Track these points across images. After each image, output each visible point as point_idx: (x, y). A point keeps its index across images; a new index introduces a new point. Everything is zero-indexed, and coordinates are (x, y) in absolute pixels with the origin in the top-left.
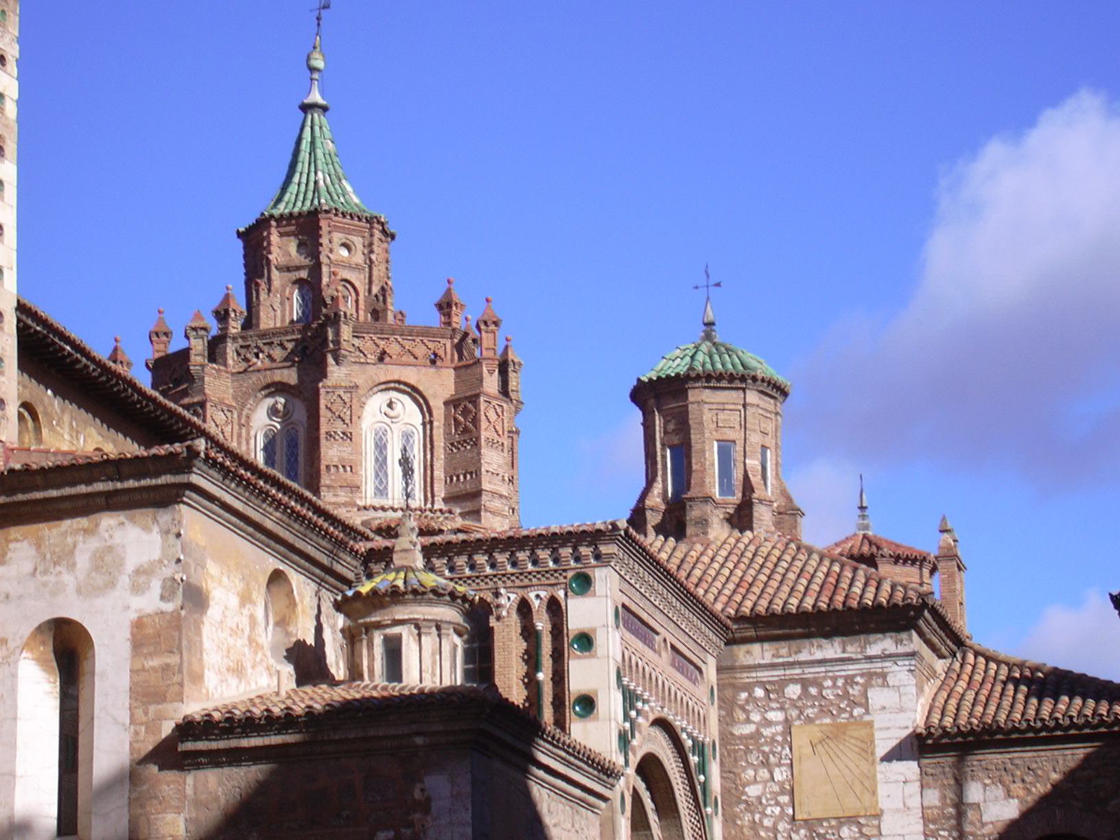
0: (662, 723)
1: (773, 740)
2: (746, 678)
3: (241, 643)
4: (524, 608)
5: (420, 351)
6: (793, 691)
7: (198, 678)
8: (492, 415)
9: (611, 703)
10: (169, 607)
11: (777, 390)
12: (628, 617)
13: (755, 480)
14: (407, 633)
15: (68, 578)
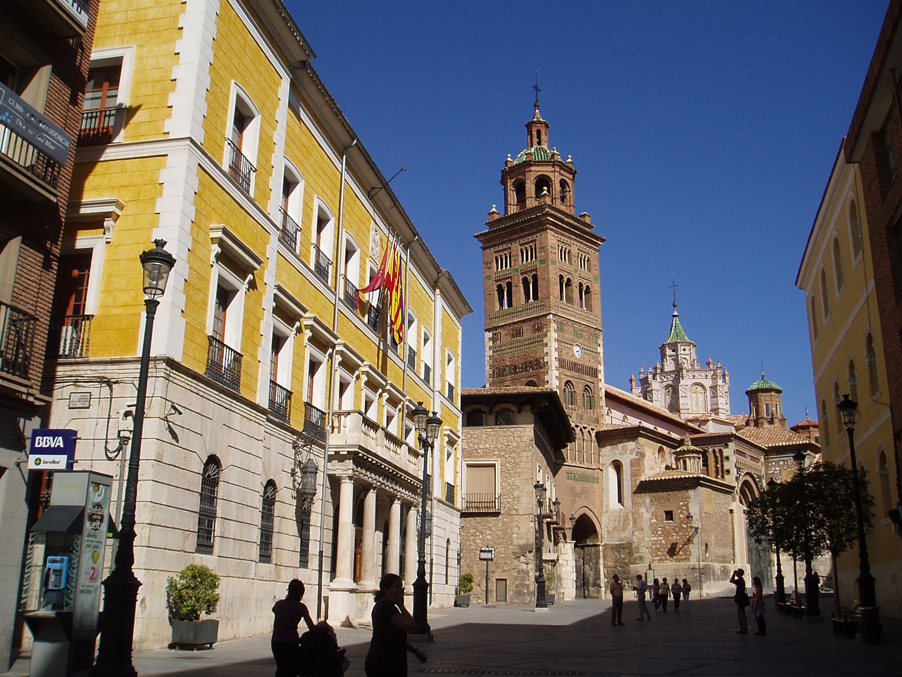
0: (748, 474)
1: (777, 474)
2: (771, 460)
3: (653, 463)
4: (714, 451)
5: (703, 374)
6: (781, 463)
7: (644, 471)
8: (721, 389)
9: (734, 471)
10: (637, 457)
11: (778, 392)
12: (738, 452)
13: (775, 413)
14: (687, 459)
15: (617, 451)
